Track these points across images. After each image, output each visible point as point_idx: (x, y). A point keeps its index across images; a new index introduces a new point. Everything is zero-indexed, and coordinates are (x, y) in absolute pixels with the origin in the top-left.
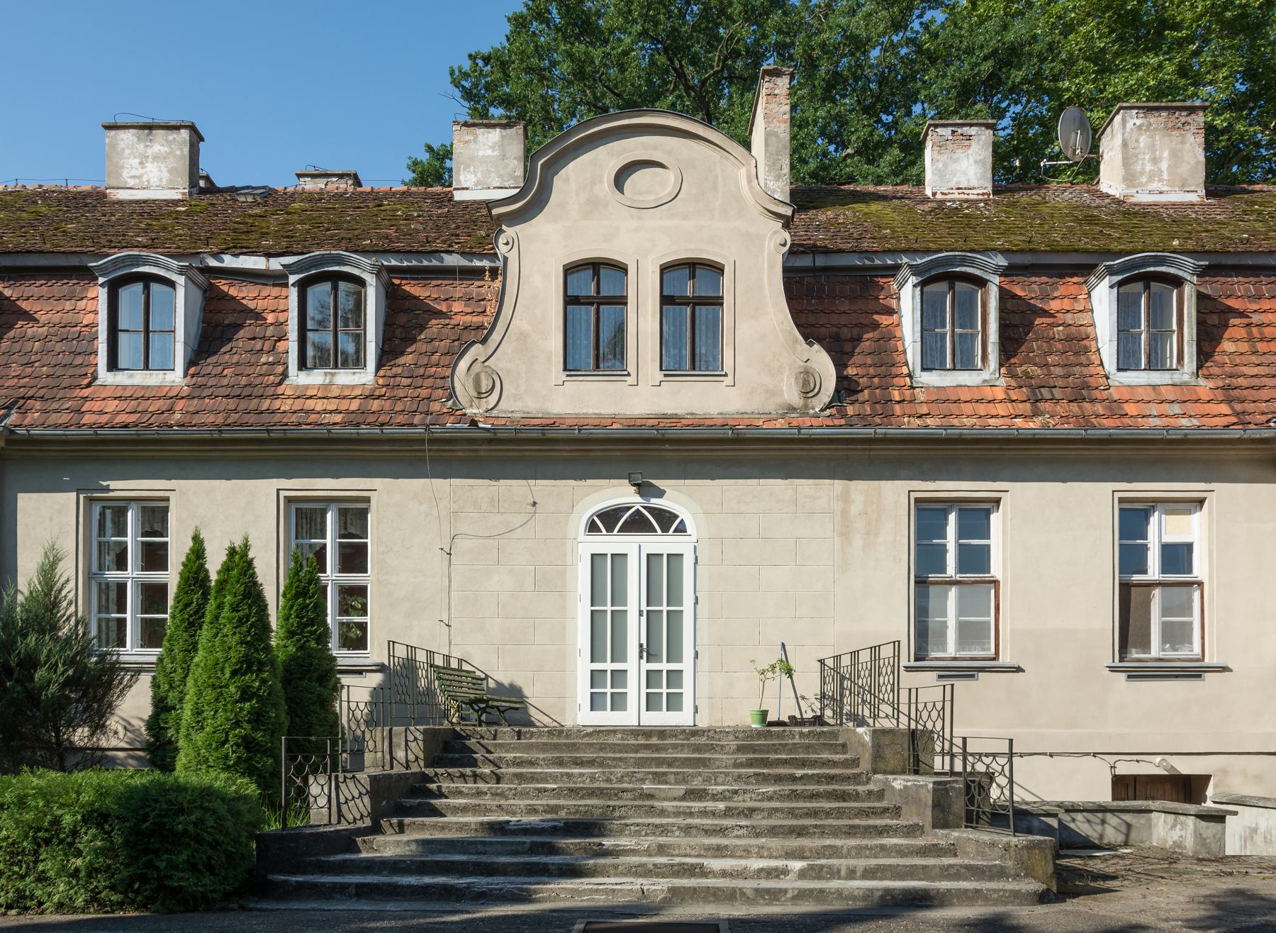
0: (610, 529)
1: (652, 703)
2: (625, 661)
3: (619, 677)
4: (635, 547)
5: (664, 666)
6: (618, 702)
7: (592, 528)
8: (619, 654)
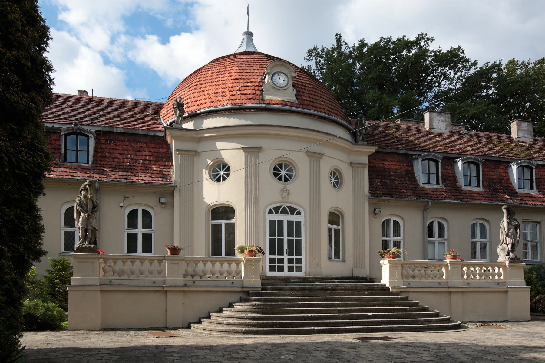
0: (277, 213)
1: (290, 269)
2: (283, 255)
3: (281, 261)
4: (286, 218)
5: (294, 257)
6: (281, 269)
7: (270, 212)
8: (281, 253)
